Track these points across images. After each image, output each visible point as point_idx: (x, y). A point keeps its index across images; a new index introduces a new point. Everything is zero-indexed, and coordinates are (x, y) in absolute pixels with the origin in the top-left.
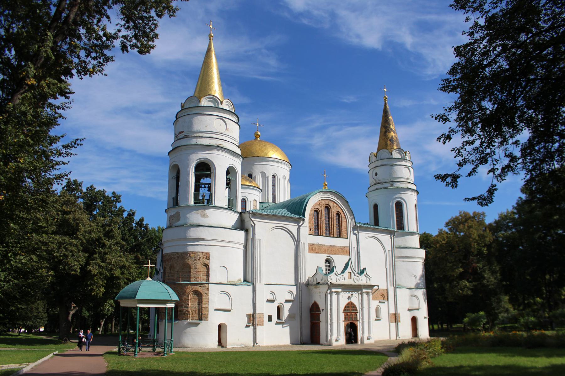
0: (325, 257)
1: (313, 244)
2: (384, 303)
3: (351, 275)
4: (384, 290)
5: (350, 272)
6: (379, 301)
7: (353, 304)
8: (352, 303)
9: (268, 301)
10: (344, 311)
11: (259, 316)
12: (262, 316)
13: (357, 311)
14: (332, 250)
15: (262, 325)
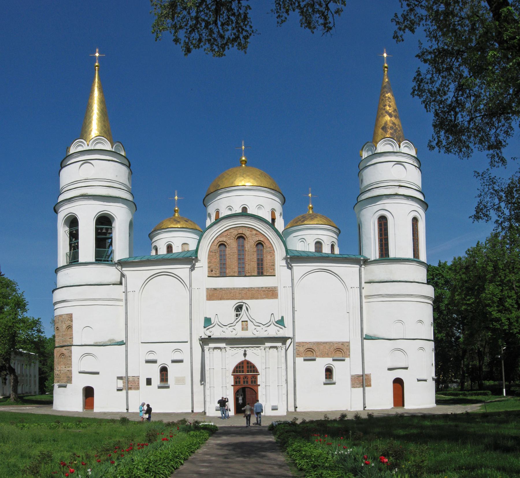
0: (234, 303)
1: (215, 289)
2: (344, 360)
3: (247, 325)
4: (343, 344)
5: (247, 321)
6: (331, 359)
7: (251, 363)
8: (248, 362)
9: (147, 362)
10: (234, 371)
11: (133, 379)
12: (136, 379)
13: (257, 371)
14: (246, 294)
15: (138, 388)
